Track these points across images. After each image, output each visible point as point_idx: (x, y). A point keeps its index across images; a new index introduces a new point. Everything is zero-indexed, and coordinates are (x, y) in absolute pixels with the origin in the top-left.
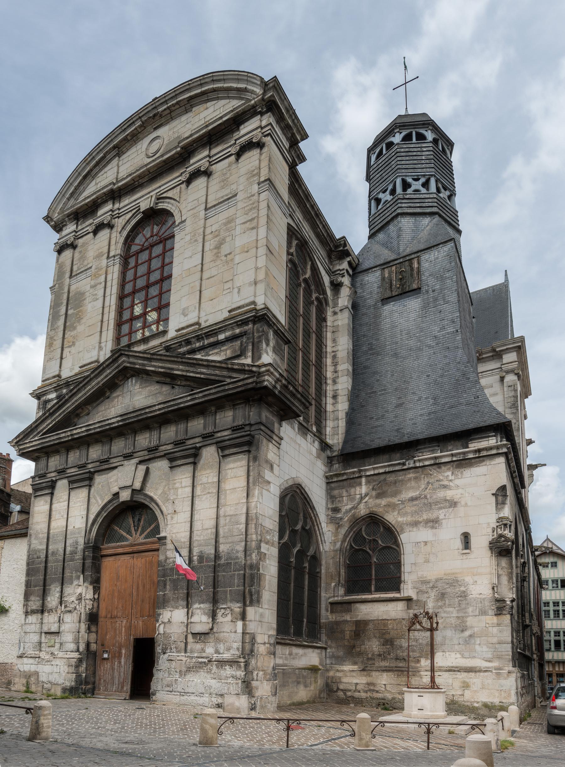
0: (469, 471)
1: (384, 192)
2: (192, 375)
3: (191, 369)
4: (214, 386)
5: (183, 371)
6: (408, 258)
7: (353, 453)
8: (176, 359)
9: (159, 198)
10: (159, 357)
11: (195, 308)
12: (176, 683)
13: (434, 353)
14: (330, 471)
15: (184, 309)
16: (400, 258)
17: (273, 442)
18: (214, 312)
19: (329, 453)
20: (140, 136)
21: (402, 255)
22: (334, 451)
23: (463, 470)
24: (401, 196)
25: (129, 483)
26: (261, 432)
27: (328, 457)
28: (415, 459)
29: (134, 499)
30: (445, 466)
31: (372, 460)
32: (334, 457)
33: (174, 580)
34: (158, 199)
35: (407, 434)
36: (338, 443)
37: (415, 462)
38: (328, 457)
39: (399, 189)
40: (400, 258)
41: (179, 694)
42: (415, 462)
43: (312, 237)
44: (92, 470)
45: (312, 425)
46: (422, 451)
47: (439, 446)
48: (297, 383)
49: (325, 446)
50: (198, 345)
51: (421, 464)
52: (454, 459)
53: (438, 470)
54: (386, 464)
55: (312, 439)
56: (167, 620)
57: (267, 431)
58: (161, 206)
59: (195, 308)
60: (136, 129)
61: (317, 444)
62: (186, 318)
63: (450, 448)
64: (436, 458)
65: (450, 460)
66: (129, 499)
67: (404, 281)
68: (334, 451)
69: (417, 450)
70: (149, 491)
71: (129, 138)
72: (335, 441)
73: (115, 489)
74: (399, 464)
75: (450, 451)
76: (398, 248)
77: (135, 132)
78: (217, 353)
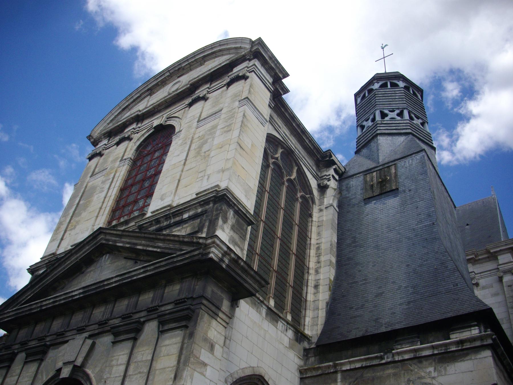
0: (453, 366)
1: (367, 120)
2: (150, 249)
3: (151, 244)
4: (165, 258)
5: (144, 245)
6: (386, 166)
7: (330, 344)
8: (140, 235)
9: (169, 118)
10: (127, 234)
11: (172, 194)
13: (413, 244)
14: (305, 364)
15: (163, 195)
16: (380, 166)
17: (218, 319)
18: (186, 194)
19: (306, 345)
20: (167, 82)
21: (380, 164)
22: (312, 343)
23: (446, 365)
24: (380, 122)
25: (72, 359)
26: (203, 307)
27: (305, 350)
28: (393, 351)
29: (74, 377)
30: (426, 360)
31: (350, 352)
32: (312, 348)
34: (167, 118)
35: (385, 324)
36: (317, 334)
37: (393, 355)
38: (305, 350)
39: (378, 118)
40: (380, 166)
42: (393, 355)
43: (299, 149)
44: (48, 343)
45: (286, 313)
46: (401, 342)
47: (418, 337)
48: (271, 269)
49: (300, 336)
50: (165, 224)
51: (400, 358)
52: (436, 352)
53: (419, 365)
54: (363, 357)
55: (284, 328)
57: (210, 306)
58: (169, 123)
59: (172, 194)
60: (165, 78)
61: (290, 333)
62: (162, 202)
63: (431, 339)
64: (415, 351)
65: (431, 353)
66: (67, 376)
67: (383, 185)
68: (312, 343)
69: (396, 342)
70: (89, 371)
71: (159, 83)
72: (314, 332)
73: (60, 364)
74: (376, 358)
75: (432, 342)
76: (378, 158)
77: (164, 80)
78: (179, 230)
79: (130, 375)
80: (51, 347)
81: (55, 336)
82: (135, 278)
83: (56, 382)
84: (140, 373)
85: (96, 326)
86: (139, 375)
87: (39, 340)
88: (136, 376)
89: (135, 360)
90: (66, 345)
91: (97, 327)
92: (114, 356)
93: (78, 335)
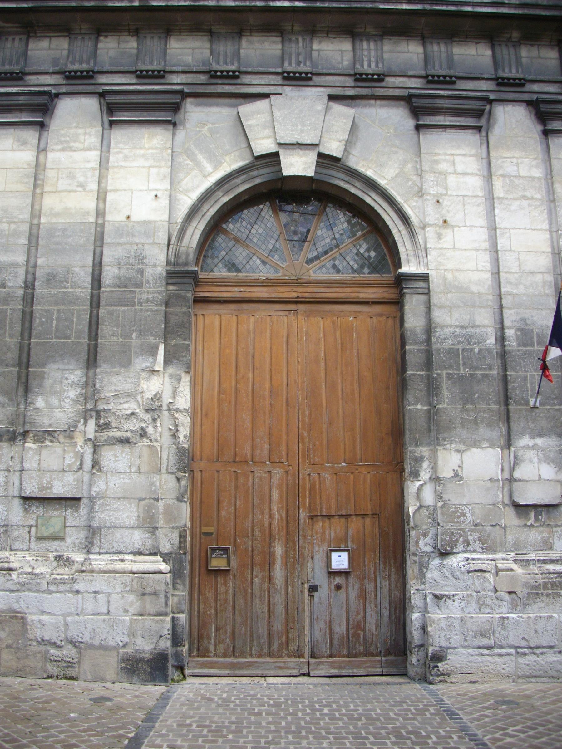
12: (503, 627)
33: (461, 379)
41: (513, 651)
56: (452, 474)
79: (499, 198)
80: (189, 100)
81: (203, 78)
82: (469, 9)
83: (257, 181)
84: (524, 197)
85: (349, 81)
86: (525, 203)
87: (138, 77)
88: (518, 203)
89: (500, 172)
90: (262, 104)
91: (352, 84)
92: (439, 154)
93: (288, 89)
